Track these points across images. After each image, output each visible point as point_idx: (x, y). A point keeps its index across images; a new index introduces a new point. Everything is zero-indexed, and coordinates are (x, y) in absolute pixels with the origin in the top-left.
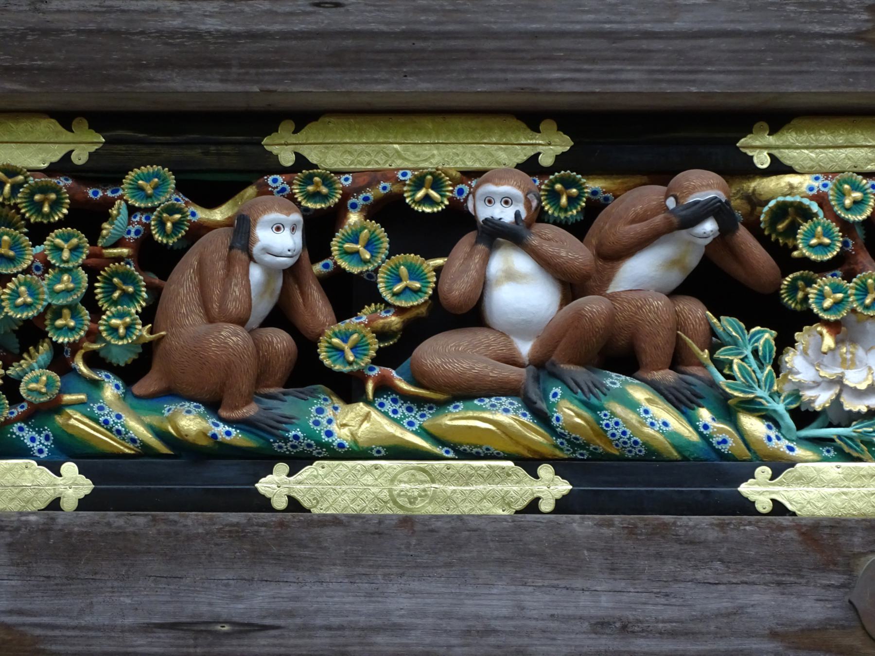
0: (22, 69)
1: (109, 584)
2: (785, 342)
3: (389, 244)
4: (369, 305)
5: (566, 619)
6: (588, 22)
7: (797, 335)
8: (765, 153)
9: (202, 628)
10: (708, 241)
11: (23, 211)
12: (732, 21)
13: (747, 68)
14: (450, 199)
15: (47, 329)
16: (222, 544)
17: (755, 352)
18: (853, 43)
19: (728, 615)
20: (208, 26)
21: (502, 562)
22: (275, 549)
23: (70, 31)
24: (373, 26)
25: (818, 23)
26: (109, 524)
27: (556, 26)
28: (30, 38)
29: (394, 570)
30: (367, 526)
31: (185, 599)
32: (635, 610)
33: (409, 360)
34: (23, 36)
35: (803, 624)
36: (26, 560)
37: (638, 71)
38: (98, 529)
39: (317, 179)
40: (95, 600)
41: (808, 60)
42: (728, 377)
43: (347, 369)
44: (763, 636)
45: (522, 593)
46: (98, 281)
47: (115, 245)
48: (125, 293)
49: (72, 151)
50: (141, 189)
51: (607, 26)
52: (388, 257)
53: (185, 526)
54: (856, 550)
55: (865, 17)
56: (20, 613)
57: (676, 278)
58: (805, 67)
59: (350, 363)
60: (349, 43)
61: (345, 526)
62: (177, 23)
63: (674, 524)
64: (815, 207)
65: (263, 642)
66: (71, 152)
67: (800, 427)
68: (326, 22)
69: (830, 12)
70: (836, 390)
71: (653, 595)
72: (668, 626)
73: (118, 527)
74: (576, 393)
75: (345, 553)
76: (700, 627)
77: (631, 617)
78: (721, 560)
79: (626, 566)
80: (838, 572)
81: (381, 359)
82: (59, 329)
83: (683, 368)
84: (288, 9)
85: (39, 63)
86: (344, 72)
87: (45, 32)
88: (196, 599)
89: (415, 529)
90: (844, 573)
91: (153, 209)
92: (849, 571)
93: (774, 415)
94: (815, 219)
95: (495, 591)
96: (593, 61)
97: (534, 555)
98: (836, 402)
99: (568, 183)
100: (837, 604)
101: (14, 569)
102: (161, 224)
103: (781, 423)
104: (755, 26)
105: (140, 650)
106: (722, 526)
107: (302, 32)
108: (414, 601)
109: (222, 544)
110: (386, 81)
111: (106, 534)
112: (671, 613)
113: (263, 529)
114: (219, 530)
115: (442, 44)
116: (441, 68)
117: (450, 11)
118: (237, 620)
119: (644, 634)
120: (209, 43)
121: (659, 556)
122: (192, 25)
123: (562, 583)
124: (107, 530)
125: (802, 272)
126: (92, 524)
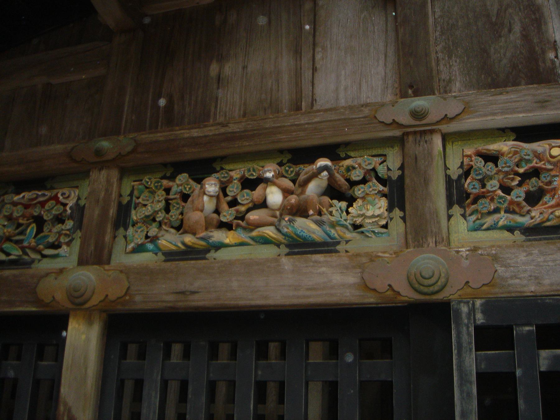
2: (350, 205)
8: (344, 153)
14: (258, 174)
17: (340, 208)
49: (166, 174)
52: (241, 191)
57: (320, 190)
59: (228, 219)
82: (158, 217)
99: (290, 167)
102: (185, 188)
104: (336, 118)
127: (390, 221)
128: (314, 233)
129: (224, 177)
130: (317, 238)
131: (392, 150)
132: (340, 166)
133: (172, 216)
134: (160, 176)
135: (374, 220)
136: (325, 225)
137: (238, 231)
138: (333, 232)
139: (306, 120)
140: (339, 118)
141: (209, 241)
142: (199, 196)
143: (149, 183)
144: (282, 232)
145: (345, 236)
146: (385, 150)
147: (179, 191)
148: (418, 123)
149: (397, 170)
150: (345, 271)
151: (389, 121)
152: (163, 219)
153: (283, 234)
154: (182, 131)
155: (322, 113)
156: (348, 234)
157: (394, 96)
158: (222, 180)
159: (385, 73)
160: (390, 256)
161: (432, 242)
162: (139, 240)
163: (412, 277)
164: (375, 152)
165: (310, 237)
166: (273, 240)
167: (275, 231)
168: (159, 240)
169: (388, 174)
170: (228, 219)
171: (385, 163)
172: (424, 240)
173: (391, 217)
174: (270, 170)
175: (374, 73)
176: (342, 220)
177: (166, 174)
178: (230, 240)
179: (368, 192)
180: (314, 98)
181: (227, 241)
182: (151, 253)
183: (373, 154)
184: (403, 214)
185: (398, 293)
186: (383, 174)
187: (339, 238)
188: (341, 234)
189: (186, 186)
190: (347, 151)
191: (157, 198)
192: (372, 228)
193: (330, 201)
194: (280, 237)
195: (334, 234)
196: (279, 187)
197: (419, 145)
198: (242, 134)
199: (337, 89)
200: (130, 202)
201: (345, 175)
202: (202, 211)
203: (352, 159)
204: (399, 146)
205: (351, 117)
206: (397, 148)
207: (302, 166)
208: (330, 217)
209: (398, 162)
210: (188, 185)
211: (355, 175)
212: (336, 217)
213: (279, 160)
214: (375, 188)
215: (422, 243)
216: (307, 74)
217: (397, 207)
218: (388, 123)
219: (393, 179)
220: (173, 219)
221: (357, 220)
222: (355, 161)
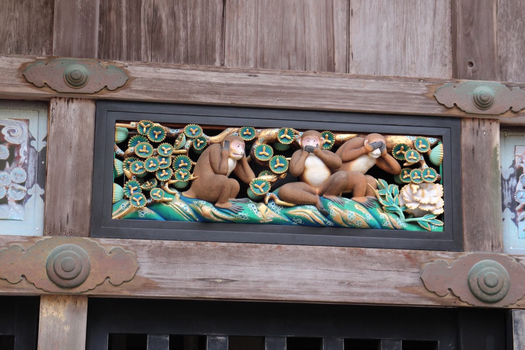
0: (151, 92)
1: (181, 265)
5: (330, 281)
6: (337, 86)
9: (212, 280)
13: (388, 104)
16: (219, 253)
18: (421, 97)
19: (382, 281)
21: (310, 261)
22: (236, 255)
23: (167, 80)
24: (268, 84)
25: (410, 90)
26: (181, 245)
27: (327, 87)
28: (153, 81)
29: (275, 263)
30: (266, 248)
31: (207, 271)
32: (352, 278)
34: (151, 81)
35: (406, 285)
36: (154, 256)
38: (177, 247)
40: (177, 270)
41: (407, 102)
44: (393, 288)
45: (316, 272)
53: (207, 246)
54: (422, 261)
55: (425, 89)
56: (151, 274)
58: (406, 104)
60: (260, 89)
61: (259, 248)
62: (203, 79)
63: (365, 250)
68: (252, 81)
71: (358, 274)
72: (363, 284)
73: (184, 246)
75: (259, 257)
76: (373, 284)
77: (351, 280)
78: (380, 263)
79: (349, 264)
80: (417, 268)
84: (240, 77)
85: (157, 90)
86: (258, 98)
87: (159, 80)
88: (210, 271)
89: (282, 249)
90: (418, 268)
92: (420, 267)
95: (307, 271)
96: (339, 99)
97: (320, 259)
101: (150, 259)
104: (390, 90)
105: (191, 287)
106: (380, 252)
107: (245, 84)
108: (281, 273)
109: (219, 253)
110: (272, 102)
111: (181, 248)
112: (364, 280)
113: (233, 248)
114: (218, 248)
115: (289, 91)
116: (290, 98)
117: (293, 80)
118: (224, 278)
119: (355, 286)
120: (214, 86)
121: (360, 261)
122: (208, 80)
123: (329, 269)
124: (181, 247)
126: (176, 245)
155: (373, 81)
157: (443, 65)
159: (434, 35)
161: (489, 246)
163: (474, 285)
172: (480, 242)
175: (420, 33)
197: (477, 135)
199: (377, 46)
215: (479, 246)
216: (340, 17)
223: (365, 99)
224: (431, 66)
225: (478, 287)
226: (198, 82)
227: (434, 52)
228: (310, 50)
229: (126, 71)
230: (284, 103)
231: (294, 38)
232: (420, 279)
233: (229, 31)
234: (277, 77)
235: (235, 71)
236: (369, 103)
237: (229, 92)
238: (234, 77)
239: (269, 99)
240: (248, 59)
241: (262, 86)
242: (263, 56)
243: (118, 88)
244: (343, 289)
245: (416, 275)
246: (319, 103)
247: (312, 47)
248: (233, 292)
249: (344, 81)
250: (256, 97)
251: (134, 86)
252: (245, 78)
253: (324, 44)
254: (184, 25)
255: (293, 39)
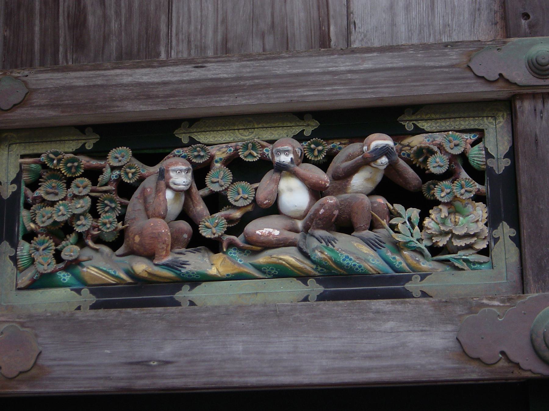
2: (424, 215)
3: (233, 177)
4: (226, 207)
6: (323, 67)
7: (431, 211)
10: (385, 167)
11: (63, 172)
12: (391, 63)
15: (73, 226)
17: (409, 219)
20: (144, 80)
24: (222, 76)
27: (307, 70)
33: (243, 233)
37: (347, 89)
39: (198, 149)
42: (396, 232)
43: (213, 237)
46: (98, 203)
47: (106, 185)
48: (111, 207)
50: (116, 158)
51: (331, 69)
52: (232, 183)
57: (371, 186)
60: (209, 84)
62: (130, 79)
64: (435, 149)
65: (173, 369)
66: (86, 143)
67: (432, 256)
68: (199, 74)
69: (438, 56)
70: (450, 236)
74: (322, 243)
81: (229, 231)
82: (78, 225)
83: (375, 230)
84: (181, 70)
87: (71, 88)
91: (122, 167)
93: (421, 251)
94: (435, 154)
96: (324, 85)
98: (450, 242)
99: (317, 145)
100: (451, 340)
102: (127, 174)
103: (424, 253)
104: (401, 64)
107: (188, 80)
110: (227, 101)
118: (160, 359)
121: (363, 319)
125: (431, 181)
127: (495, 244)
128: (367, 261)
129: (199, 156)
130: (371, 269)
131: (494, 122)
132: (404, 146)
133: (105, 224)
134: (74, 150)
135: (468, 241)
136: (384, 248)
137: (231, 253)
138: (398, 261)
139: (348, 66)
140: (405, 64)
141: (180, 271)
142: (158, 190)
143: (55, 162)
144: (312, 258)
145: (417, 266)
146: (481, 122)
147: (114, 178)
148: (541, 82)
149: (503, 157)
150: (427, 328)
151: (494, 76)
152: (89, 230)
153: (313, 262)
154: (118, 71)
155: (375, 54)
156: (423, 264)
157: (492, 24)
158: (194, 160)
160: (502, 305)
162: (46, 267)
163: (539, 341)
164: (465, 124)
165: (360, 267)
166: (296, 271)
167: (300, 257)
168: (83, 266)
169: (488, 164)
170: (214, 234)
171: (481, 145)
173: (495, 237)
174: (288, 151)
176: (414, 239)
177: (84, 145)
178: (217, 270)
179: (458, 196)
180: (352, 20)
181: (213, 271)
182: (68, 289)
183: (462, 127)
184: (516, 232)
185: (517, 365)
186: (479, 163)
187: (409, 269)
188: (413, 263)
189: (128, 170)
190: (416, 120)
191: (73, 190)
192: (464, 255)
193: (389, 205)
194: (307, 266)
195: (400, 263)
196: (303, 180)
197: (542, 117)
198: (234, 83)
200: (16, 195)
201: (413, 161)
202: (164, 218)
203: (425, 135)
204: (505, 116)
205: (427, 64)
206: (501, 119)
207: (337, 143)
208: (394, 235)
209: (504, 143)
210: (130, 168)
211: (437, 165)
212: (404, 235)
213: (297, 130)
214: (468, 189)
217: (505, 221)
218: (492, 79)
219: (497, 172)
220: (108, 228)
221: (439, 242)
222: (431, 140)
223: (365, 82)
224: (474, 27)
225: (544, 345)
226: (122, 85)
227: (477, 6)
228: (293, 25)
229: (24, 81)
230: (246, 99)
231: (270, 10)
232: (456, 340)
233: (178, 13)
234: (235, 65)
235: (174, 62)
236: (371, 86)
237: (166, 93)
238: (173, 72)
239: (222, 97)
240: (205, 48)
241: (212, 80)
242: (225, 40)
243: (15, 105)
244: (338, 364)
245: (451, 334)
246: (297, 94)
247: (296, 21)
248: (173, 378)
249: (332, 59)
250: (205, 96)
251: (37, 99)
252: (187, 71)
253: (315, 14)
254: (116, 12)
255: (268, 12)
